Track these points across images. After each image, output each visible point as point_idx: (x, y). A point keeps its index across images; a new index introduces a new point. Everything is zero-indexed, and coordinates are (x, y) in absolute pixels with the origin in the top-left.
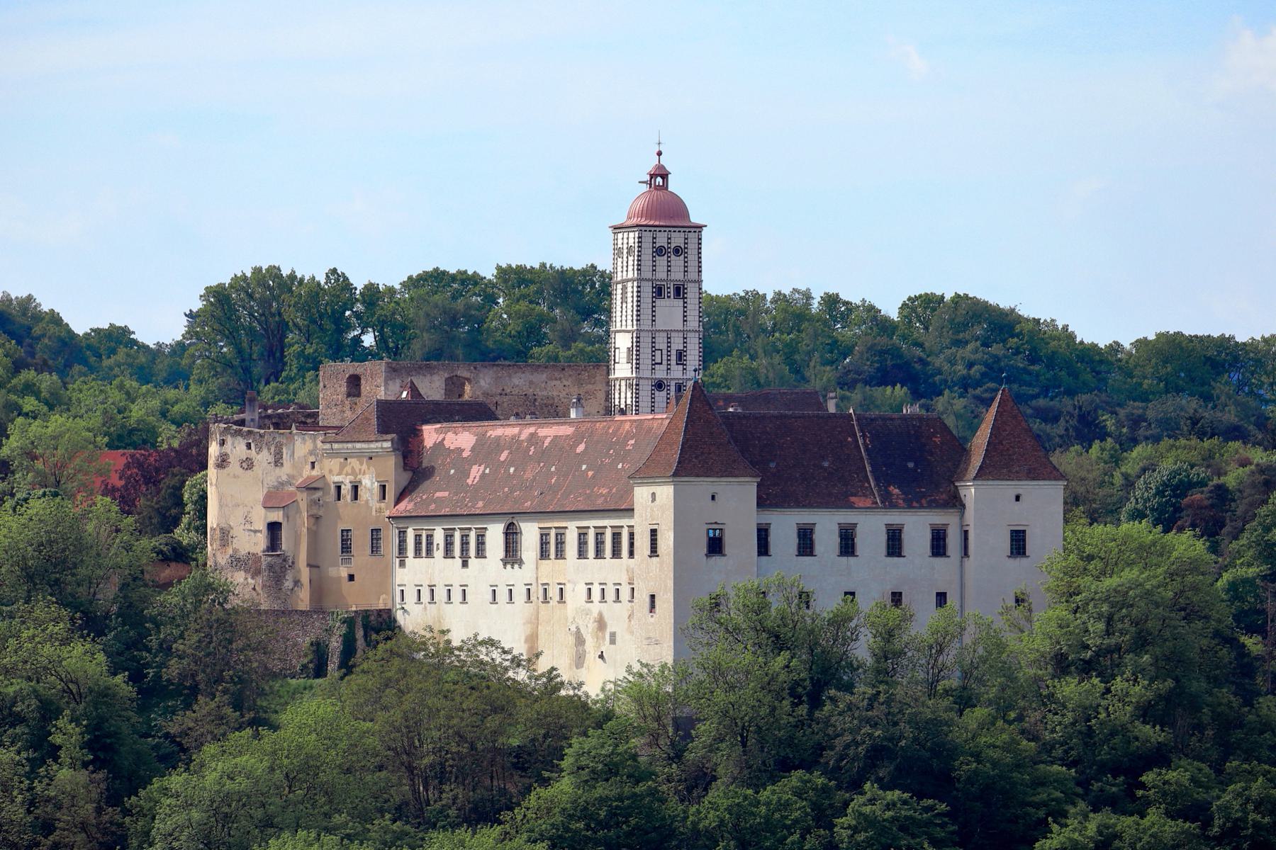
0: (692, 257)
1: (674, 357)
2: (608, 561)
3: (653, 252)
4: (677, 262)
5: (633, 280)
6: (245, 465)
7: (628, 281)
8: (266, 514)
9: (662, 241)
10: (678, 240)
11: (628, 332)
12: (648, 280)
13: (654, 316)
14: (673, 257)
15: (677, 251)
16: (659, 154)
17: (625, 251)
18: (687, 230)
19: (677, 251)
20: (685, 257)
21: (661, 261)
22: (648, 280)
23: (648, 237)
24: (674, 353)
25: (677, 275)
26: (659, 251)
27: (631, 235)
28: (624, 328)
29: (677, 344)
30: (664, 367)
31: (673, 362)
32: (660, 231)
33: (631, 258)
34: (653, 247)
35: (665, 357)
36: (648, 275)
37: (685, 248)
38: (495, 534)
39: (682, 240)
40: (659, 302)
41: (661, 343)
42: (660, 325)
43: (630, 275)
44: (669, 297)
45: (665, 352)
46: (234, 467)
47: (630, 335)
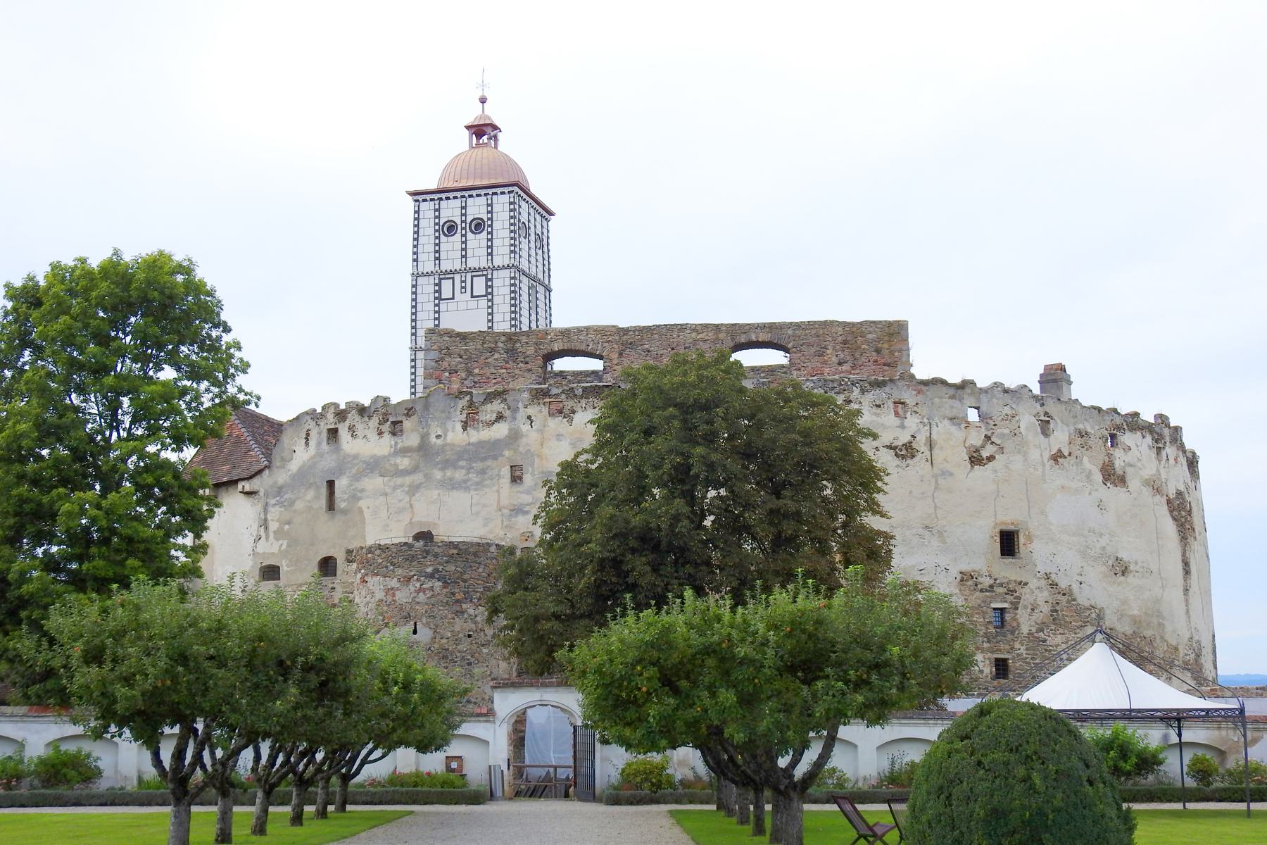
3: (436, 231)
4: (477, 243)
8: (417, 758)
9: (451, 210)
12: (428, 275)
13: (413, 328)
14: (470, 235)
15: (478, 226)
18: (490, 191)
19: (478, 226)
20: (489, 233)
21: (451, 245)
22: (428, 275)
23: (428, 209)
26: (451, 228)
32: (448, 198)
34: (436, 224)
36: (428, 266)
37: (489, 219)
39: (484, 209)
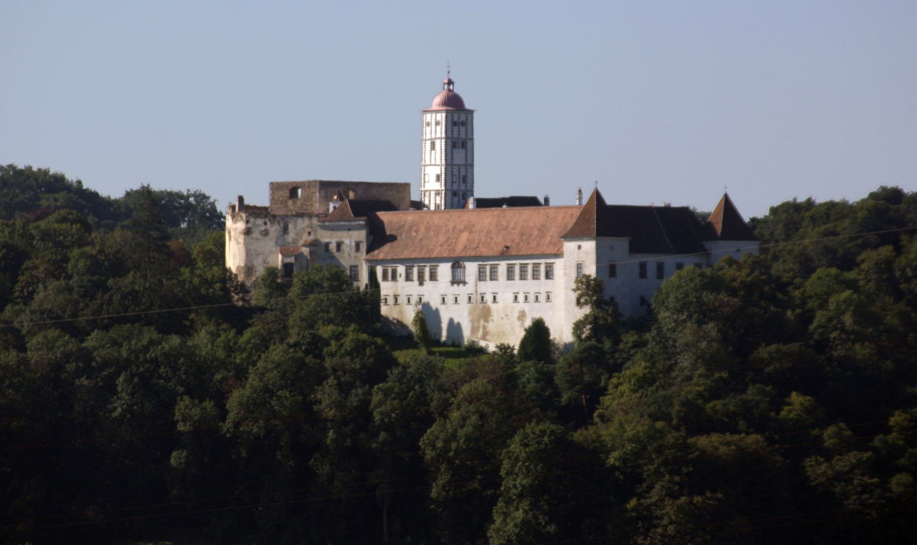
0: (469, 127)
1: (461, 179)
2: (428, 283)
4: (463, 129)
5: (441, 138)
6: (263, 233)
7: (436, 138)
10: (463, 118)
11: (439, 165)
16: (449, 72)
17: (434, 124)
24: (461, 177)
25: (463, 136)
27: (439, 115)
28: (433, 163)
29: (463, 173)
30: (457, 184)
31: (461, 182)
33: (439, 128)
35: (458, 179)
38: (401, 269)
40: (455, 150)
41: (456, 172)
42: (455, 162)
43: (438, 135)
44: (459, 147)
45: (457, 176)
46: (256, 234)
47: (439, 167)
